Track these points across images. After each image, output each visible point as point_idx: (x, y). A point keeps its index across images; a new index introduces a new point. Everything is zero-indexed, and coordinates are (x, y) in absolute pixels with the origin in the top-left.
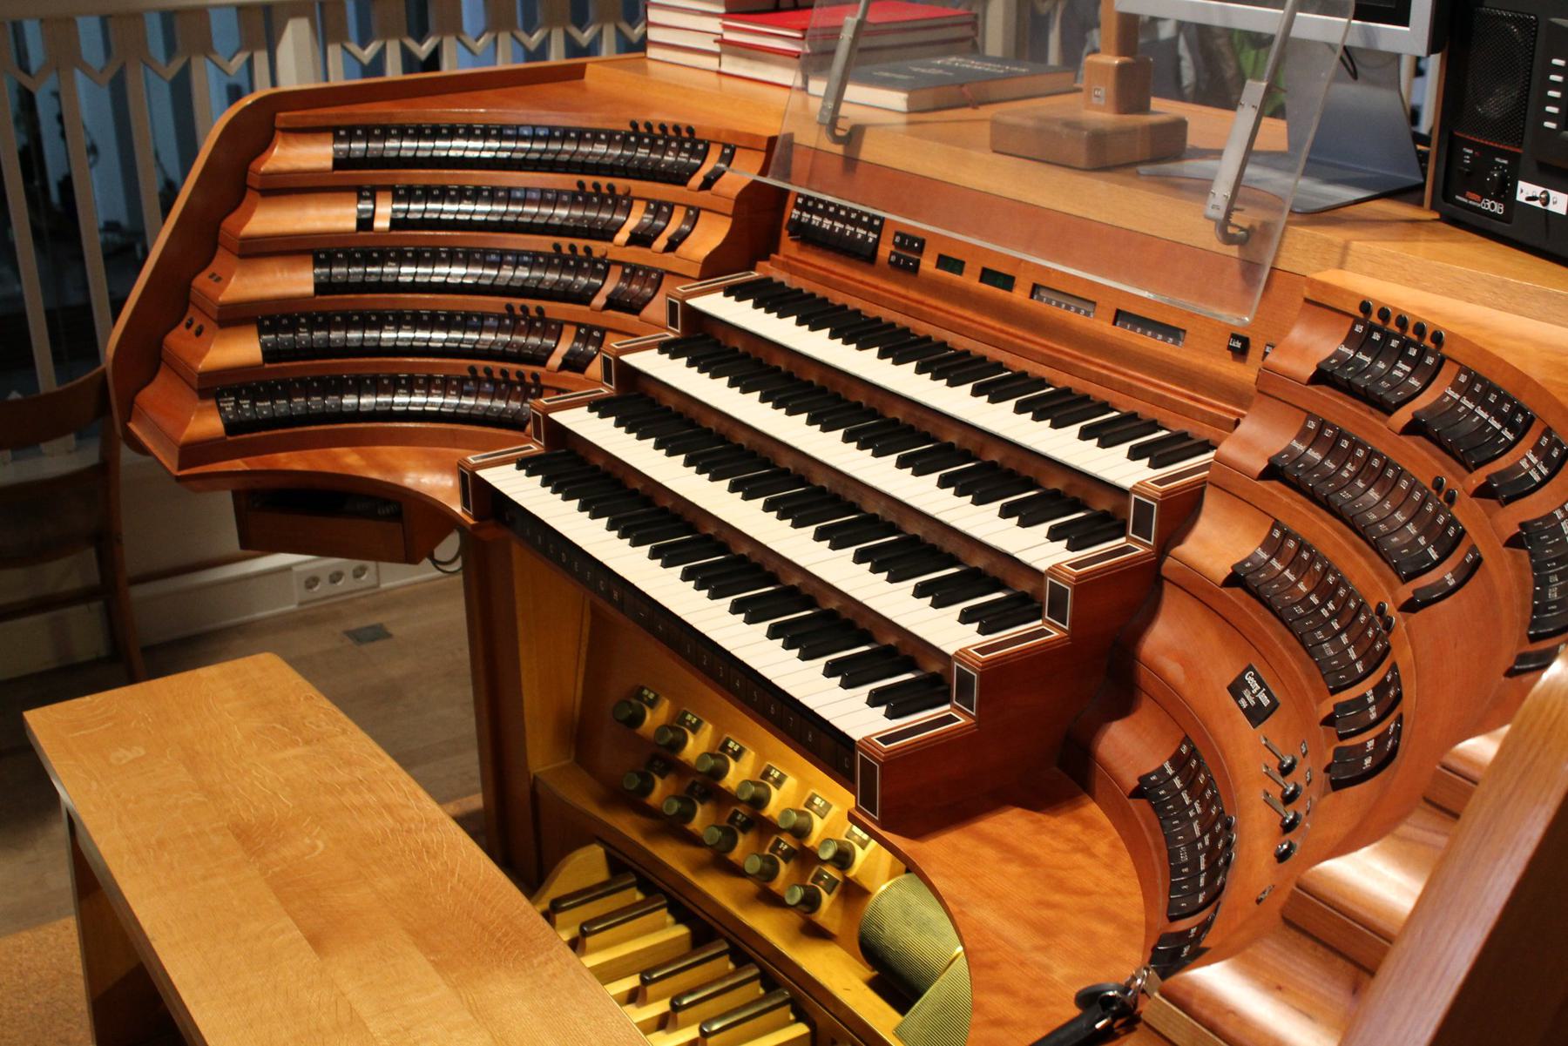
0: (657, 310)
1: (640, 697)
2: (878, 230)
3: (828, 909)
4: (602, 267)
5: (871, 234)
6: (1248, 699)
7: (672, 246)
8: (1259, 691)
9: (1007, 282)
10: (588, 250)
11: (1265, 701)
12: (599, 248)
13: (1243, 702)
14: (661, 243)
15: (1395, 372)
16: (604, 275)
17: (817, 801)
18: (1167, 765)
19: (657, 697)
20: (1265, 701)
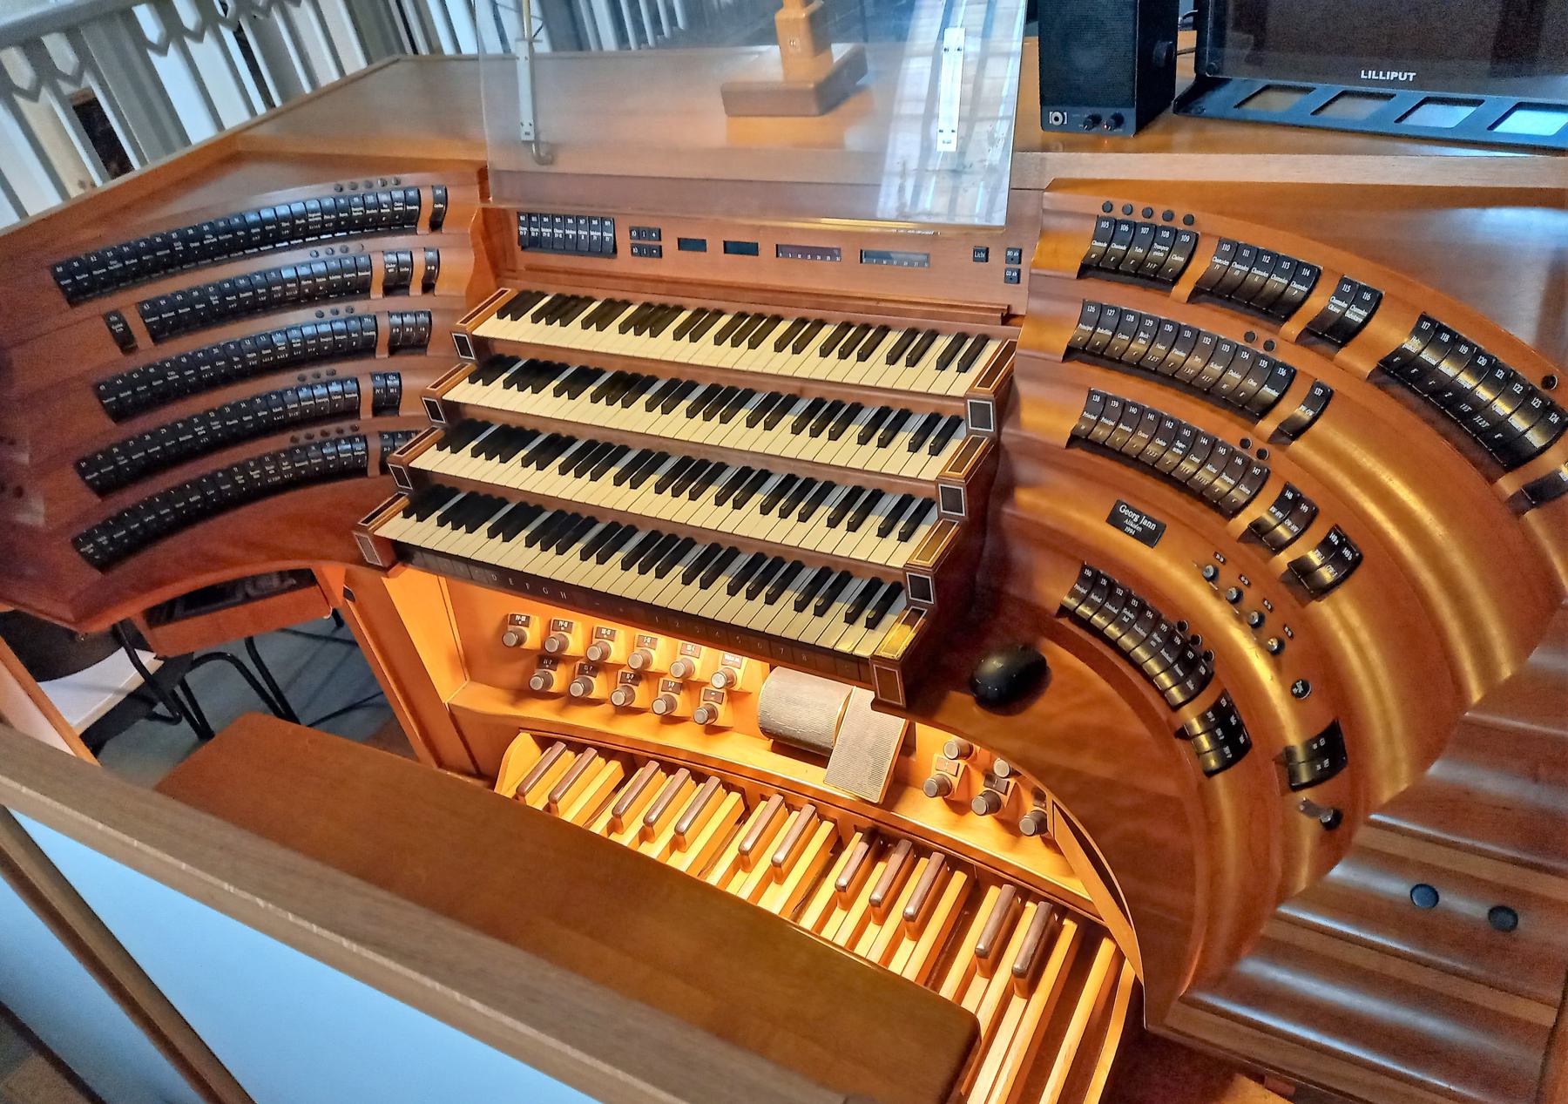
3: (724, 716)
6: (1132, 526)
8: (1140, 519)
9: (751, 249)
13: (1128, 529)
18: (1077, 587)
19: (528, 618)
20: (1153, 527)
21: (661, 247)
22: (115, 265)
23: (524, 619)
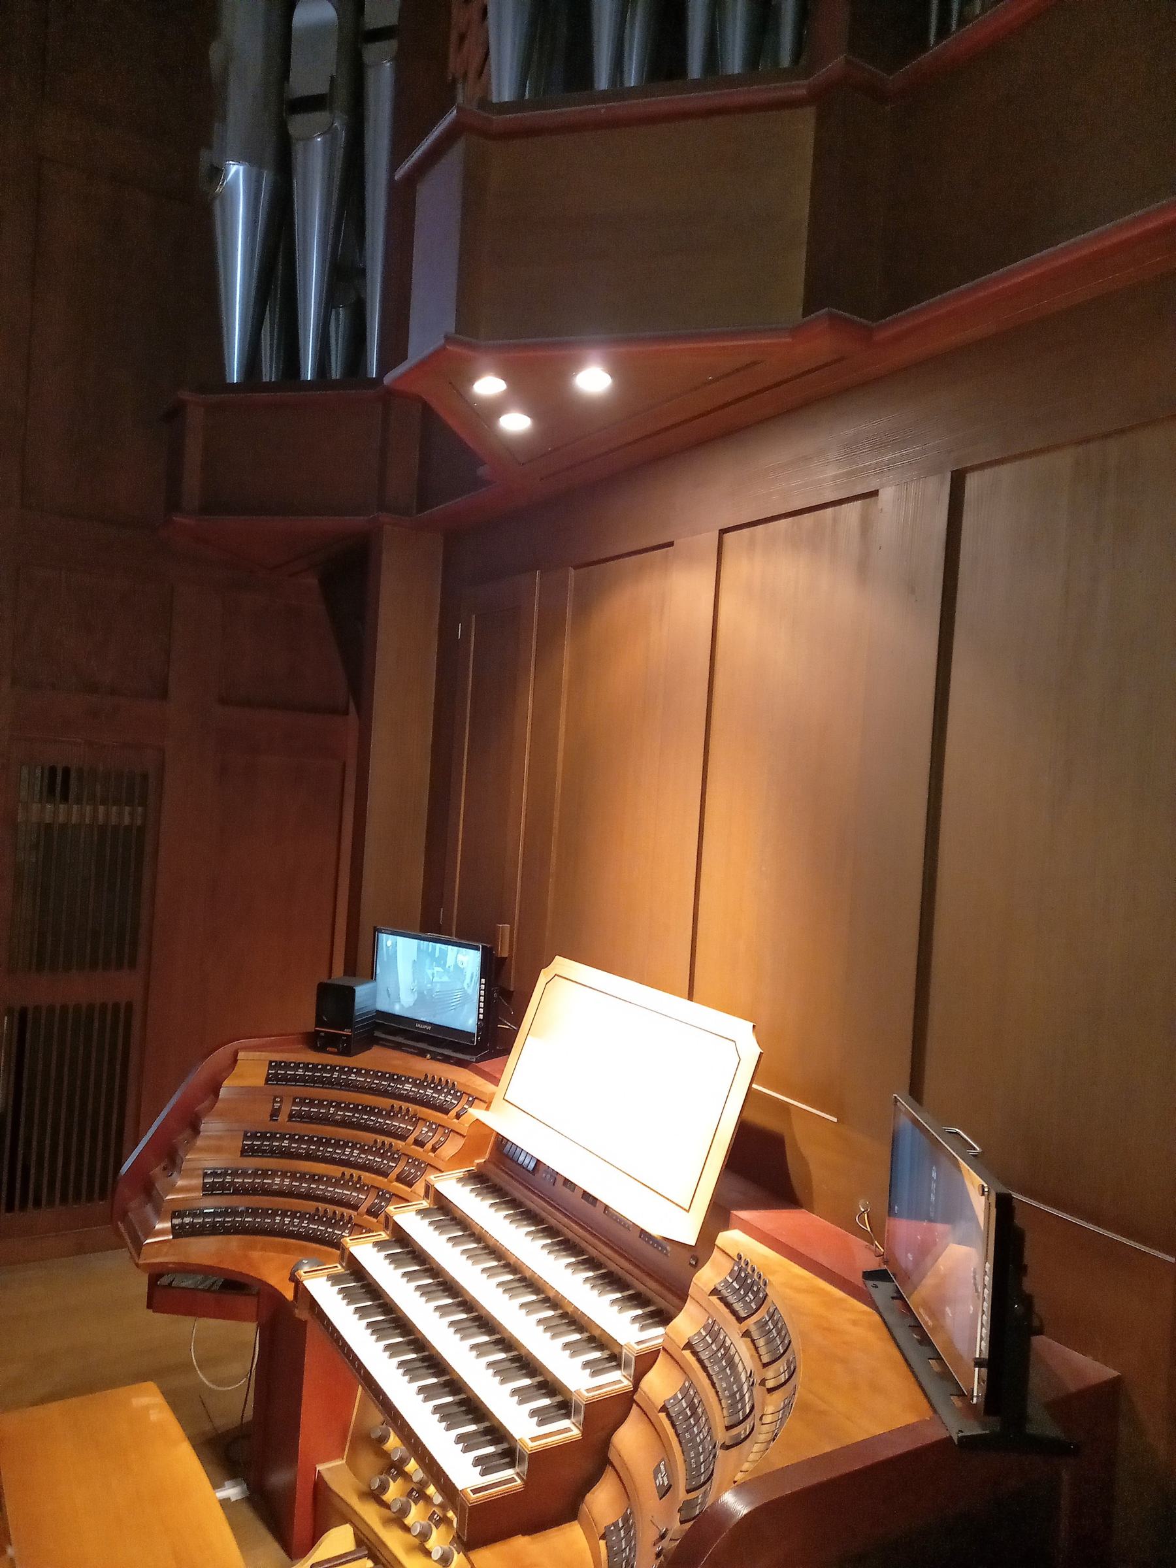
0: (419, 1187)
7: (434, 1149)
10: (391, 1145)
12: (400, 1144)
14: (429, 1146)
16: (397, 1161)
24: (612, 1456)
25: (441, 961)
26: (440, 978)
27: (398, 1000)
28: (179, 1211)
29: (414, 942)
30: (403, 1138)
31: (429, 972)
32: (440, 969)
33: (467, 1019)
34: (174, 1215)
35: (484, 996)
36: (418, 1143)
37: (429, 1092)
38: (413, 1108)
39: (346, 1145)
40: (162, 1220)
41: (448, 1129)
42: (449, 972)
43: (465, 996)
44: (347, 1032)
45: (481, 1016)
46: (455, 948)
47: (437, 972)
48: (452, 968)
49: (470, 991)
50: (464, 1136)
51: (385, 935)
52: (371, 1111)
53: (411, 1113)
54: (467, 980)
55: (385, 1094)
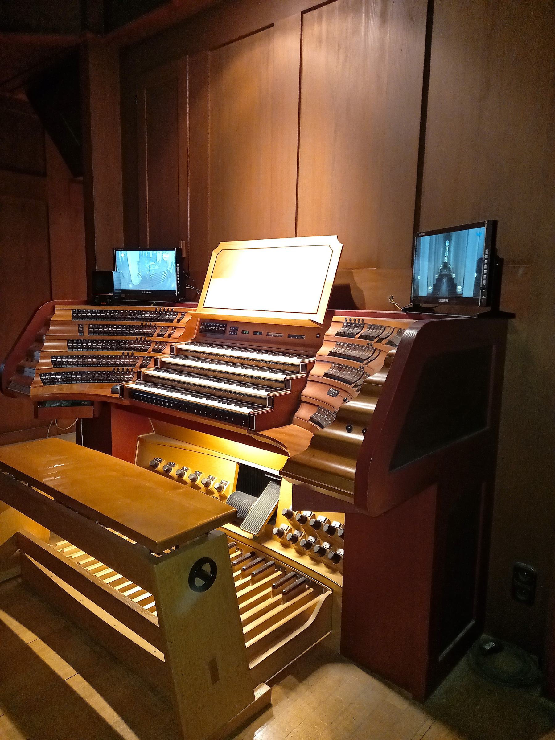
1: (156, 460)
2: (226, 327)
4: (149, 343)
5: (223, 328)
6: (332, 393)
11: (336, 392)
15: (354, 330)
16: (150, 344)
17: (211, 477)
18: (316, 413)
20: (336, 392)
21: (237, 332)
22: (89, 314)
23: (160, 460)
24: (303, 399)
25: (155, 260)
26: (154, 267)
27: (131, 281)
28: (43, 374)
29: (137, 253)
30: (151, 335)
31: (148, 266)
32: (153, 263)
33: (171, 285)
34: (41, 375)
35: (179, 272)
36: (160, 335)
37: (159, 315)
38: (153, 323)
39: (121, 342)
40: (37, 377)
41: (174, 327)
42: (158, 264)
43: (169, 275)
44: (111, 294)
45: (179, 282)
46: (161, 252)
47: (152, 265)
48: (160, 262)
49: (171, 271)
50: (184, 328)
51: (119, 251)
52: (131, 327)
53: (152, 324)
54: (170, 266)
55: (137, 319)
